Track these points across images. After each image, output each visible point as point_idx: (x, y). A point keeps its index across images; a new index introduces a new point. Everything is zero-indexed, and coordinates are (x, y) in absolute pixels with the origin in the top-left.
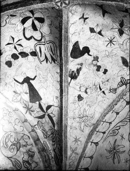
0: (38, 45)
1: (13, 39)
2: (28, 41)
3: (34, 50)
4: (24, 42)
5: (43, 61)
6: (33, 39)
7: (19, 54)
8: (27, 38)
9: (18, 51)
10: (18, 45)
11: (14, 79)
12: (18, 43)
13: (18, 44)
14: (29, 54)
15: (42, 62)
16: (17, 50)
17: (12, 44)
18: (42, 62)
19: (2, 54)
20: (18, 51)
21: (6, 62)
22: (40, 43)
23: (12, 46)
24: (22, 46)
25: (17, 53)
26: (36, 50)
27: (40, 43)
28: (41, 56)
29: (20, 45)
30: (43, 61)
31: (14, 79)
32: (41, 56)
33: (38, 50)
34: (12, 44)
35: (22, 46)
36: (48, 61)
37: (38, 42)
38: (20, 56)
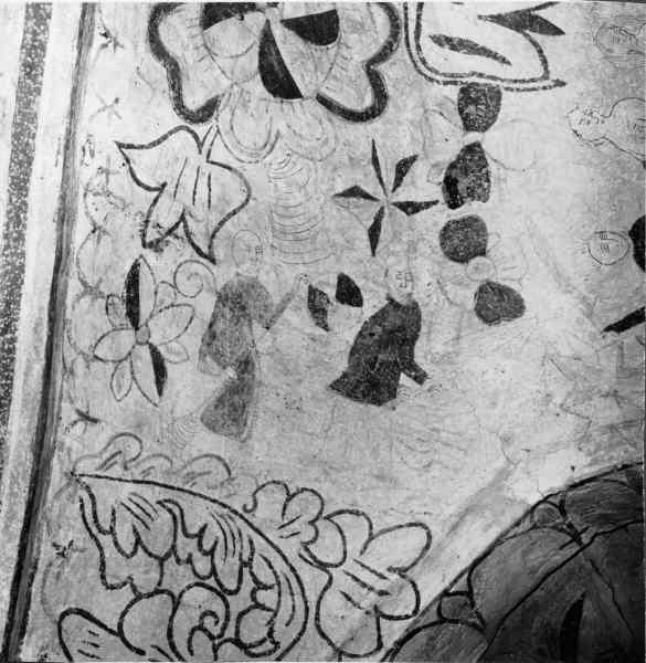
0: (419, 48)
1: (354, 192)
2: (390, 109)
3: (453, 92)
4: (395, 134)
5: (545, 62)
6: (382, 68)
7: (453, 205)
8: (372, 108)
9: (435, 203)
10: (398, 182)
11: (609, 329)
12: (389, 176)
13: (391, 188)
14: (473, 137)
15: (553, 76)
16: (428, 205)
17: (381, 211)
18: (553, 76)
19: (415, 305)
20: (435, 203)
21: (480, 315)
22: (412, 26)
23: (394, 222)
24: (414, 159)
25: (441, 215)
26: (452, 79)
27: (412, 26)
28: (504, 61)
29: (403, 168)
30: (545, 62)
31: (609, 329)
32: (504, 61)
33: (464, 63)
34: (381, 211)
35: (414, 159)
36: (537, 12)
37: (402, 36)
38: (470, 209)
